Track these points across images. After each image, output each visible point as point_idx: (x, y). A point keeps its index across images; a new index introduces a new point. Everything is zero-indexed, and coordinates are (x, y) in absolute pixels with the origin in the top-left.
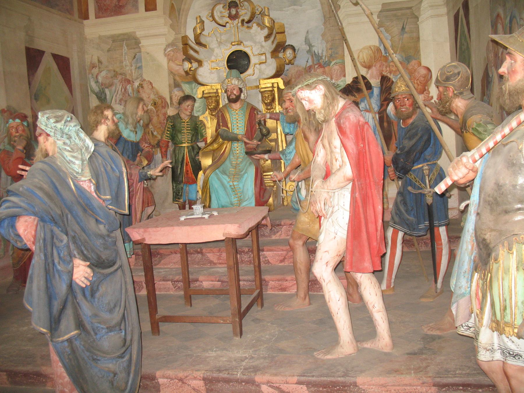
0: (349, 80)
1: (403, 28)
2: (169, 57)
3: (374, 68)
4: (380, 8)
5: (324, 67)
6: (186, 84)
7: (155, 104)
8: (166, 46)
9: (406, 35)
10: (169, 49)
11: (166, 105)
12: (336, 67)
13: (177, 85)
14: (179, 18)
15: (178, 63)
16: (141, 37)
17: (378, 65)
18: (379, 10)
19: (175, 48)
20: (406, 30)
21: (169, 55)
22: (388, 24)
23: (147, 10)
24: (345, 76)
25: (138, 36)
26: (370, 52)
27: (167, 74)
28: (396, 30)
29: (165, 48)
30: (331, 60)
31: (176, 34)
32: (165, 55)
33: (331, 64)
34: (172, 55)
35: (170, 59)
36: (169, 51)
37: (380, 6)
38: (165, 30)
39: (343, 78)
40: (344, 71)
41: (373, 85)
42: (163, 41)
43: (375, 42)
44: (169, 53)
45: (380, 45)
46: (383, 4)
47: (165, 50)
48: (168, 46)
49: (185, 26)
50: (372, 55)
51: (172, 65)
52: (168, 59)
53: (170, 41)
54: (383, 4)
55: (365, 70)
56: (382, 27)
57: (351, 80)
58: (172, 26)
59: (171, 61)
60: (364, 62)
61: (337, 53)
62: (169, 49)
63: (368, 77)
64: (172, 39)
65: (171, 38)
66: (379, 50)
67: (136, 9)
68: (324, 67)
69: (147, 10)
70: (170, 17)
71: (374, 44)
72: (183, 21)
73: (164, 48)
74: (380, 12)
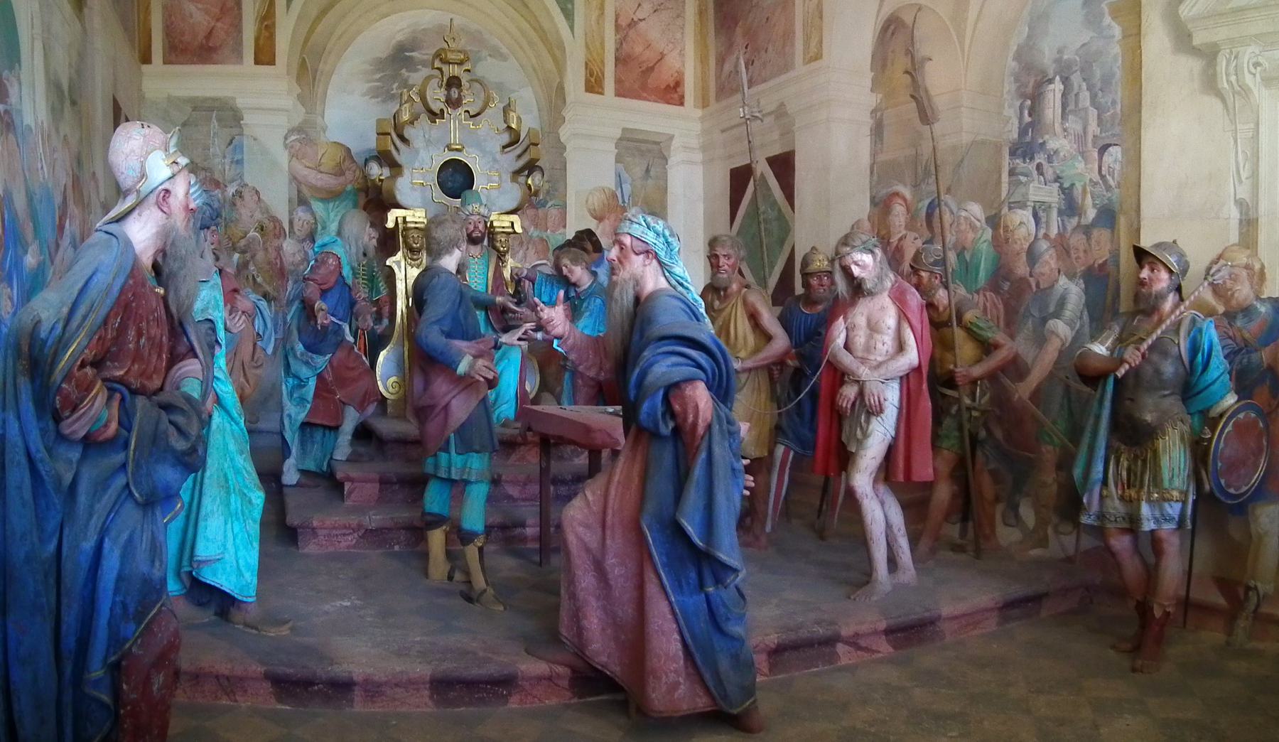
0: (570, 235)
1: (648, 171)
2: (293, 151)
3: (606, 221)
4: (618, 134)
5: (537, 209)
6: (319, 201)
7: (262, 230)
8: (289, 131)
9: (650, 182)
10: (293, 138)
11: (282, 232)
12: (554, 212)
13: (302, 202)
14: (313, 87)
15: (308, 164)
16: (246, 108)
17: (612, 218)
18: (619, 136)
19: (304, 136)
20: (652, 173)
21: (292, 147)
22: (629, 159)
23: (258, 62)
24: (565, 227)
25: (239, 106)
26: (603, 196)
27: (287, 180)
28: (639, 171)
29: (287, 134)
30: (548, 198)
31: (307, 113)
32: (286, 146)
33: (548, 206)
34: (297, 148)
35: (293, 156)
36: (293, 141)
37: (620, 132)
38: (288, 102)
39: (562, 230)
40: (564, 219)
41: (603, 246)
42: (282, 123)
43: (610, 183)
44: (293, 143)
45: (617, 189)
46: (624, 130)
47: (286, 138)
48: (292, 131)
49: (324, 103)
50: (606, 202)
51: (295, 162)
52: (290, 152)
53: (296, 123)
54: (624, 130)
55: (595, 221)
56: (621, 163)
57: (574, 235)
58: (300, 98)
59: (294, 159)
60: (595, 210)
61: (556, 190)
62: (293, 138)
63: (598, 233)
64: (300, 120)
65: (297, 120)
66: (614, 196)
67: (238, 56)
68: (537, 209)
69: (257, 62)
70: (299, 79)
71: (609, 186)
72: (320, 90)
73: (284, 134)
74: (621, 139)
